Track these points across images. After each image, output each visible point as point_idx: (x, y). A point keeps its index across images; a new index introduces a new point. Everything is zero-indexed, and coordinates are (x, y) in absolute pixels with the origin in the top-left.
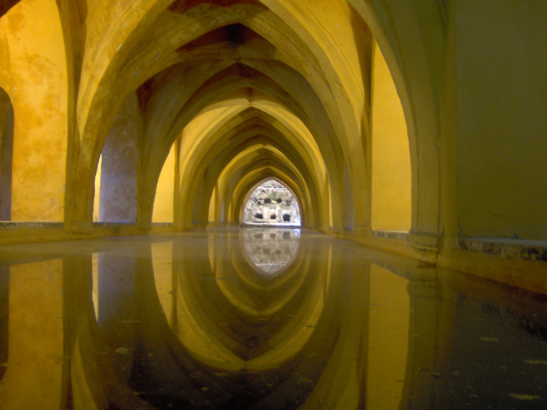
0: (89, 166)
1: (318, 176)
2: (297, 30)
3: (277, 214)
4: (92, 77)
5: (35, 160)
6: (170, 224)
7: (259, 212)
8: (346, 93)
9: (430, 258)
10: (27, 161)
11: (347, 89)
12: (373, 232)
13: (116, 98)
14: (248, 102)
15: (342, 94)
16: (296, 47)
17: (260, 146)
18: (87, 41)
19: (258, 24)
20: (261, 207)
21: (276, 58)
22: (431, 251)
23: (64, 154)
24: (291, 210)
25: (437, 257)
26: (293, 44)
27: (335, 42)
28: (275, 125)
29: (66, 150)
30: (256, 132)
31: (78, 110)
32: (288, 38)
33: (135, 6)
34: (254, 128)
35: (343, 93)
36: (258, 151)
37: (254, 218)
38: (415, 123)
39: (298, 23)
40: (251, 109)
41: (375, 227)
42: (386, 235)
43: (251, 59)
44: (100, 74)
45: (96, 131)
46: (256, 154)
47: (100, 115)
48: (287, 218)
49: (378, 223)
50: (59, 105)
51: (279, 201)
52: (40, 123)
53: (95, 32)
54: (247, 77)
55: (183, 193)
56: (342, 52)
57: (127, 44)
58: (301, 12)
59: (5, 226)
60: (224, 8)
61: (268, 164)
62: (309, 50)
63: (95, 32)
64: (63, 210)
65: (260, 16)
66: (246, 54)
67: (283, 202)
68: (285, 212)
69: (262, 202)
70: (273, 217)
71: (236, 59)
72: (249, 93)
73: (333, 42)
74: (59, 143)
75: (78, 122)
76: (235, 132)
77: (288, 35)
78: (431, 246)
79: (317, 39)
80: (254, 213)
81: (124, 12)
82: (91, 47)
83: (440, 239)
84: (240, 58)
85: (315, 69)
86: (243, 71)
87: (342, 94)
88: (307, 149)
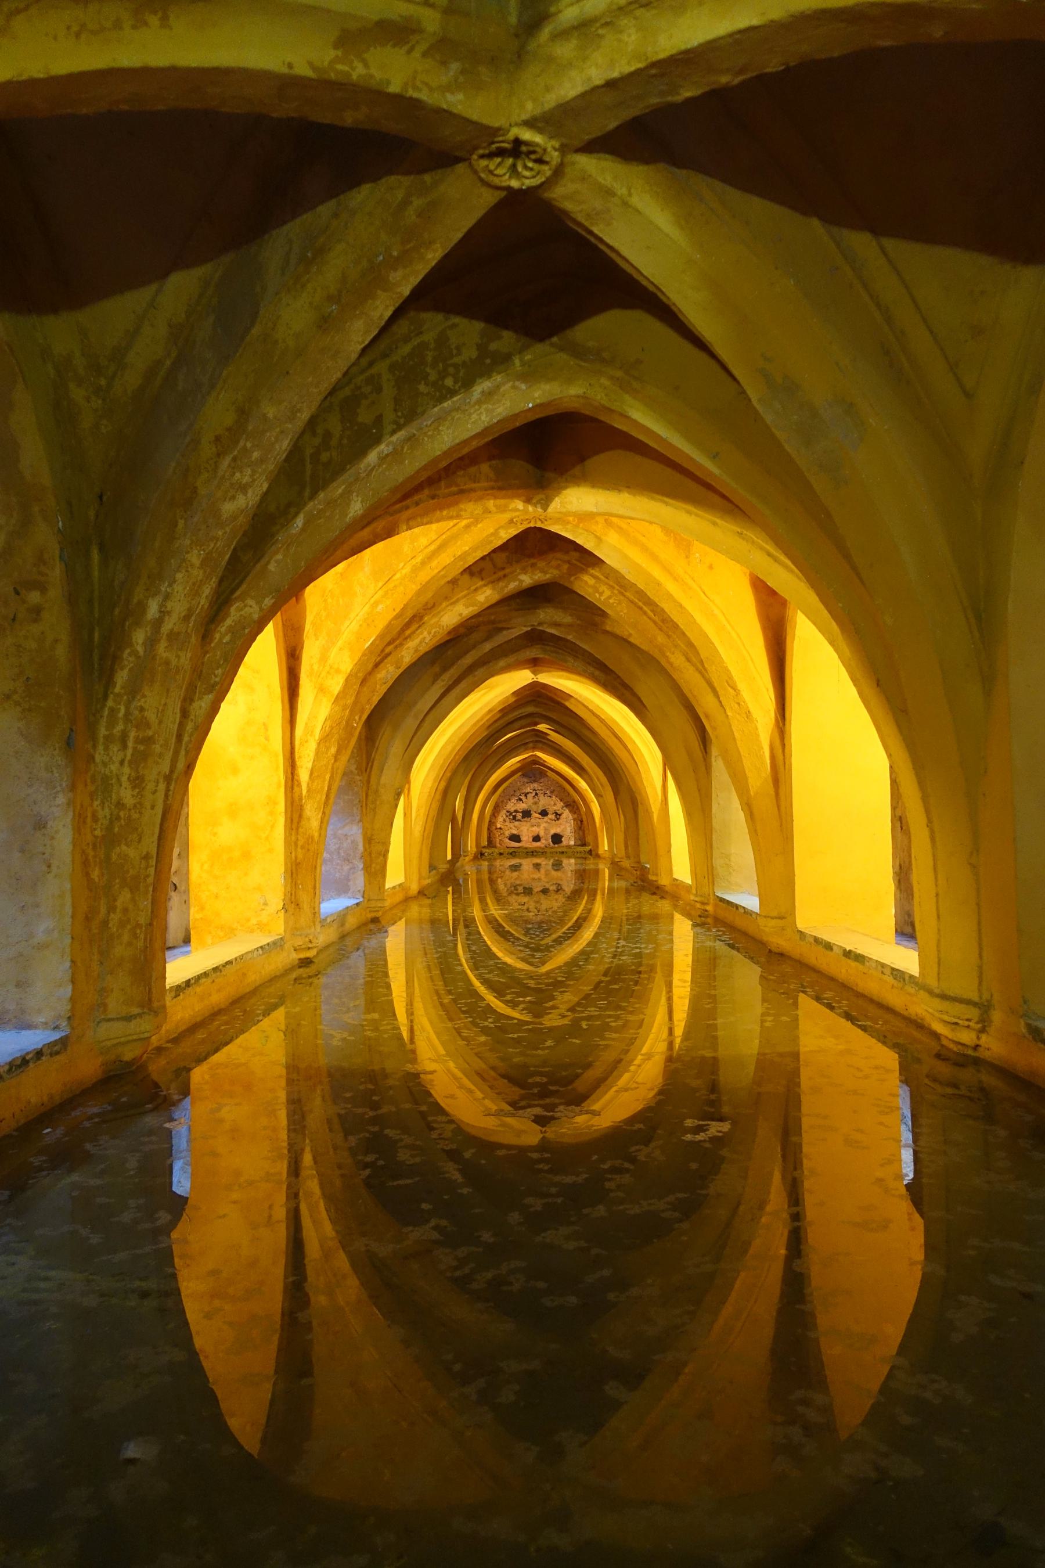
0: (316, 835)
1: (649, 791)
4: (322, 690)
5: (229, 833)
9: (967, 1037)
10: (215, 834)
13: (357, 718)
15: (739, 704)
16: (655, 623)
18: (308, 627)
21: (608, 628)
22: (968, 1027)
23: (281, 821)
25: (978, 1038)
26: (650, 618)
27: (727, 620)
29: (283, 815)
30: (530, 709)
32: (641, 608)
33: (398, 575)
38: (930, 821)
39: (670, 596)
42: (835, 948)
43: (557, 625)
44: (336, 684)
45: (328, 777)
47: (333, 750)
49: (810, 918)
50: (267, 739)
52: (235, 770)
53: (324, 614)
54: (543, 647)
55: (417, 829)
56: (738, 635)
57: (381, 637)
58: (676, 579)
60: (533, 561)
61: (534, 748)
62: (676, 626)
63: (324, 614)
64: (282, 914)
65: (592, 571)
72: (534, 664)
73: (725, 623)
74: (272, 801)
75: (298, 763)
76: (499, 716)
77: (640, 604)
78: (968, 1020)
79: (699, 618)
80: (507, 833)
81: (380, 584)
82: (317, 639)
83: (985, 1008)
84: (540, 624)
85: (688, 660)
86: (535, 637)
87: (739, 704)
88: (630, 747)
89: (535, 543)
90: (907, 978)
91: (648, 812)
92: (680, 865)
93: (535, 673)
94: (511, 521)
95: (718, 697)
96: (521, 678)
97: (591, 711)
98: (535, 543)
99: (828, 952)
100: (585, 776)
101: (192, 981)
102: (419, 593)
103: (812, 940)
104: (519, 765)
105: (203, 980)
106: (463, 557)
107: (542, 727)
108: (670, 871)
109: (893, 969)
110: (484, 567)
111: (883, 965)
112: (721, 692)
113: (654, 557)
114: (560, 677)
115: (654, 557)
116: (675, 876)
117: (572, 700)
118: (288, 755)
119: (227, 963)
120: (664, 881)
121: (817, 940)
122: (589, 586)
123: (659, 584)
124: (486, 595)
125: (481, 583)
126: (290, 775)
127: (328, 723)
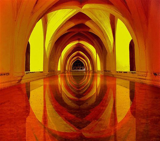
2: (98, 25)
7: (75, 67)
11: (109, 38)
12: (117, 72)
17: (78, 52)
19: (88, 24)
28: (84, 47)
34: (79, 48)
41: (118, 70)
51: (79, 65)
55: (62, 64)
66: (81, 30)
68: (81, 67)
70: (78, 69)
91: (94, 62)
92: (99, 67)
102: (63, 22)
106: (70, 16)
112: (106, 38)
113: (97, 18)
115: (97, 18)
120: (96, 71)
121: (120, 72)
123: (97, 21)
124: (72, 25)
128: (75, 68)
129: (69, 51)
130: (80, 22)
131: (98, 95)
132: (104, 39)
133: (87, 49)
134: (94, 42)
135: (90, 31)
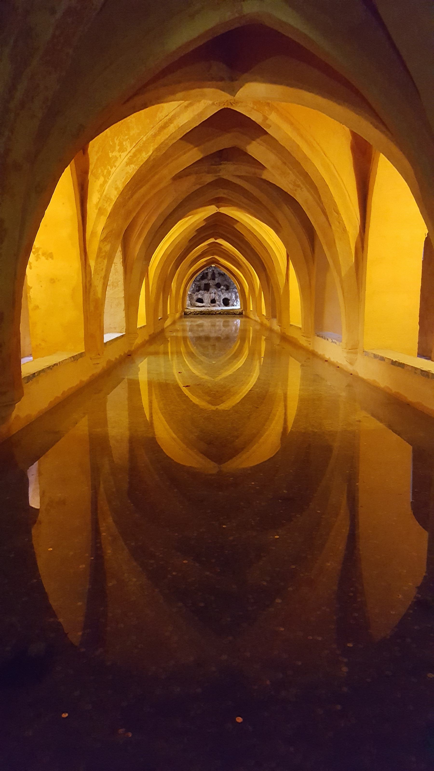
3: (217, 298)
6: (144, 326)
7: (200, 296)
8: (343, 221)
14: (217, 209)
15: (339, 223)
17: (212, 240)
20: (200, 292)
21: (264, 177)
24: (230, 294)
31: (87, 243)
35: (340, 221)
36: (208, 245)
37: (194, 302)
40: (218, 214)
42: (386, 360)
46: (207, 247)
48: (226, 302)
51: (218, 286)
59: (51, 369)
67: (222, 287)
68: (223, 297)
69: (202, 286)
70: (213, 301)
71: (219, 176)
72: (218, 201)
89: (227, 120)
90: (430, 375)
93: (218, 207)
94: (213, 104)
95: (327, 219)
96: (211, 210)
97: (249, 230)
98: (227, 120)
99: (382, 362)
100: (241, 270)
101: (36, 374)
103: (372, 356)
104: (205, 263)
105: (41, 374)
107: (220, 241)
108: (289, 321)
109: (422, 371)
110: (194, 136)
111: (416, 369)
114: (233, 210)
116: (291, 323)
117: (238, 224)
118: (83, 249)
119: (54, 365)
122: (255, 149)
125: (192, 146)
126: (84, 261)
127: (106, 232)
128: (200, 300)
129: (175, 246)
130: (225, 141)
131: (289, 429)
132: (322, 218)
133: (248, 238)
134: (280, 216)
135: (265, 176)
